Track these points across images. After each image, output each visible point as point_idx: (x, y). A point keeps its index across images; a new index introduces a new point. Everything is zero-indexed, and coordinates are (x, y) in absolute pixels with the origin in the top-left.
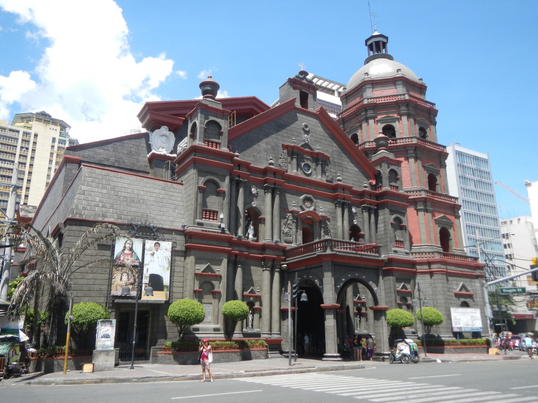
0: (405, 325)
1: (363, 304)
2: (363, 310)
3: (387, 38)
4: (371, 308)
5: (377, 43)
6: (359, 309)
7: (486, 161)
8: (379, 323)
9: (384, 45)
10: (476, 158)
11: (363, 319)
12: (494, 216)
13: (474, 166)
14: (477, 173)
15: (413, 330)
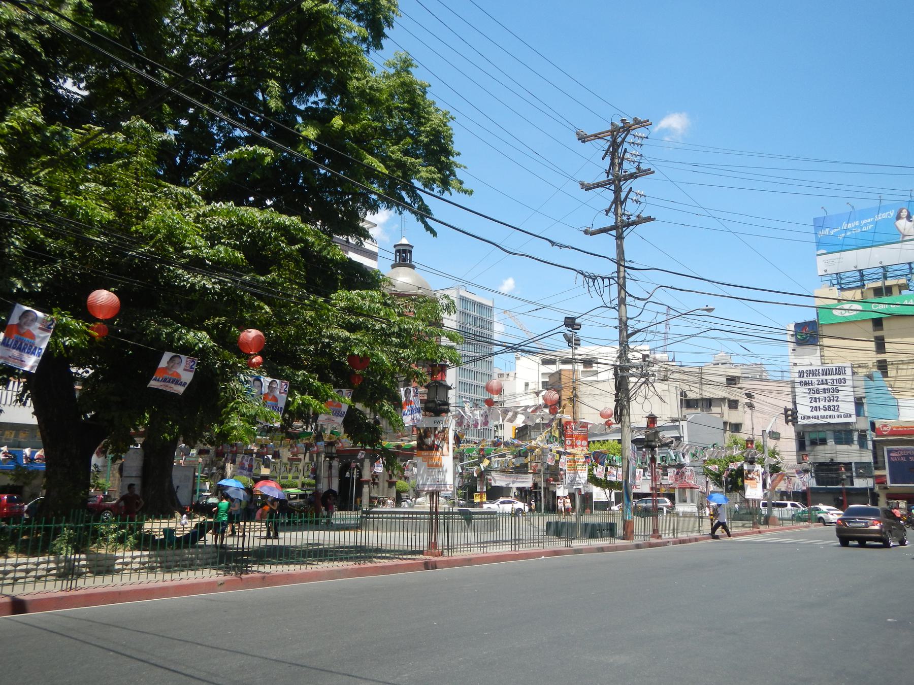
0: (404, 491)
1: (377, 476)
2: (376, 481)
3: (412, 247)
4: (387, 481)
5: (405, 251)
6: (374, 480)
7: (490, 309)
8: (391, 490)
9: (410, 252)
10: (480, 305)
11: (376, 486)
12: (489, 372)
13: (476, 314)
14: (479, 323)
15: (407, 494)
